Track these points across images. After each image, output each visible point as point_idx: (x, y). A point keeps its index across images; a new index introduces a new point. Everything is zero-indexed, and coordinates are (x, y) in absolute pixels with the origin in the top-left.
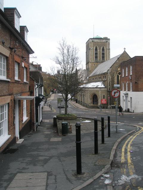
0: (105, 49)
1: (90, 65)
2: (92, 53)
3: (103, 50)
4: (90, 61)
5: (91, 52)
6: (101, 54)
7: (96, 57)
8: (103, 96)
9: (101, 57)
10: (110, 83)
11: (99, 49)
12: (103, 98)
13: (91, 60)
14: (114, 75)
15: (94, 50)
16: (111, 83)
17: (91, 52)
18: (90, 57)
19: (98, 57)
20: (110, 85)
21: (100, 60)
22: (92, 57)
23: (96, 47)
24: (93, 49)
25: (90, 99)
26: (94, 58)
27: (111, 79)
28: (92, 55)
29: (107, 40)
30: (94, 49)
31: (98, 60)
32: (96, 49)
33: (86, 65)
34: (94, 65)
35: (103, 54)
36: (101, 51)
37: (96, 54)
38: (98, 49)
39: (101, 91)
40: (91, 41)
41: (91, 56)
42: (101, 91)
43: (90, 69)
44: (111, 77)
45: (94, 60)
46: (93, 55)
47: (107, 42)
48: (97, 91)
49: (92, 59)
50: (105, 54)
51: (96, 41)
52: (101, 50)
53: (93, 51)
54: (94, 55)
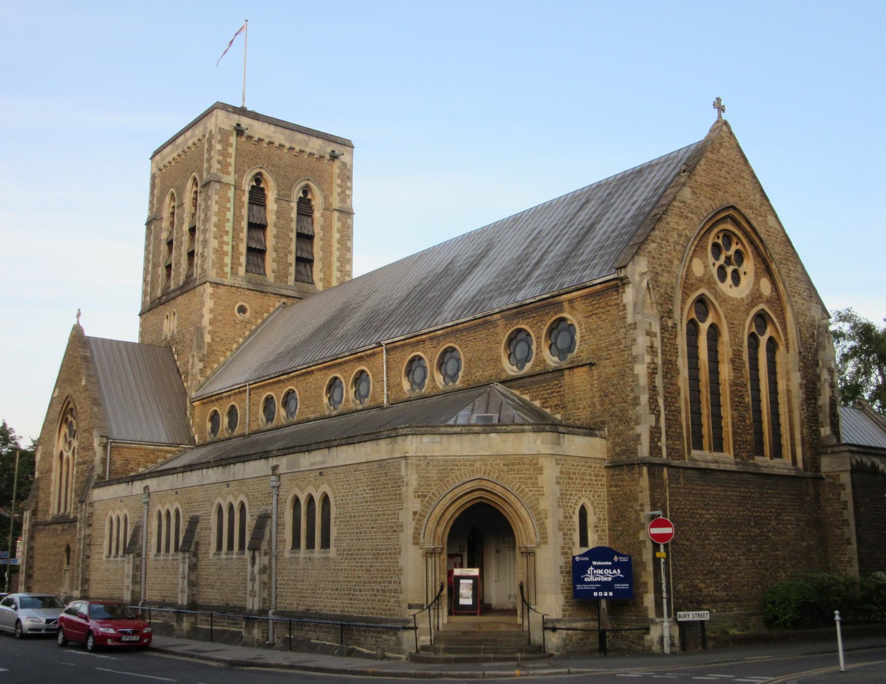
0: (317, 202)
1: (209, 304)
2: (230, 215)
3: (305, 208)
4: (212, 275)
5: (223, 209)
6: (293, 235)
7: (256, 253)
8: (576, 518)
9: (292, 259)
10: (652, 374)
11: (278, 200)
12: (576, 537)
13: (221, 266)
14: (670, 311)
15: (246, 198)
16: (659, 381)
17: (223, 209)
18: (214, 243)
19: (270, 256)
20: (653, 401)
21: (281, 276)
22: (228, 248)
23: (258, 178)
24: (237, 187)
25: (431, 553)
26: (243, 259)
27: (657, 343)
28: (229, 226)
29: (338, 149)
30: (247, 188)
31: (270, 277)
32: (257, 196)
33: (137, 320)
34: (242, 310)
35: (305, 238)
36: (294, 214)
37: (257, 227)
38: (271, 195)
39: (560, 459)
40: (226, 121)
41: (219, 236)
42: (560, 459)
43: (208, 338)
44: (656, 328)
45: (242, 270)
46: (236, 230)
47: (334, 157)
48: (515, 462)
49: (228, 260)
50: (317, 243)
51: (259, 130)
52: (294, 205)
53: (238, 206)
54: (244, 235)
